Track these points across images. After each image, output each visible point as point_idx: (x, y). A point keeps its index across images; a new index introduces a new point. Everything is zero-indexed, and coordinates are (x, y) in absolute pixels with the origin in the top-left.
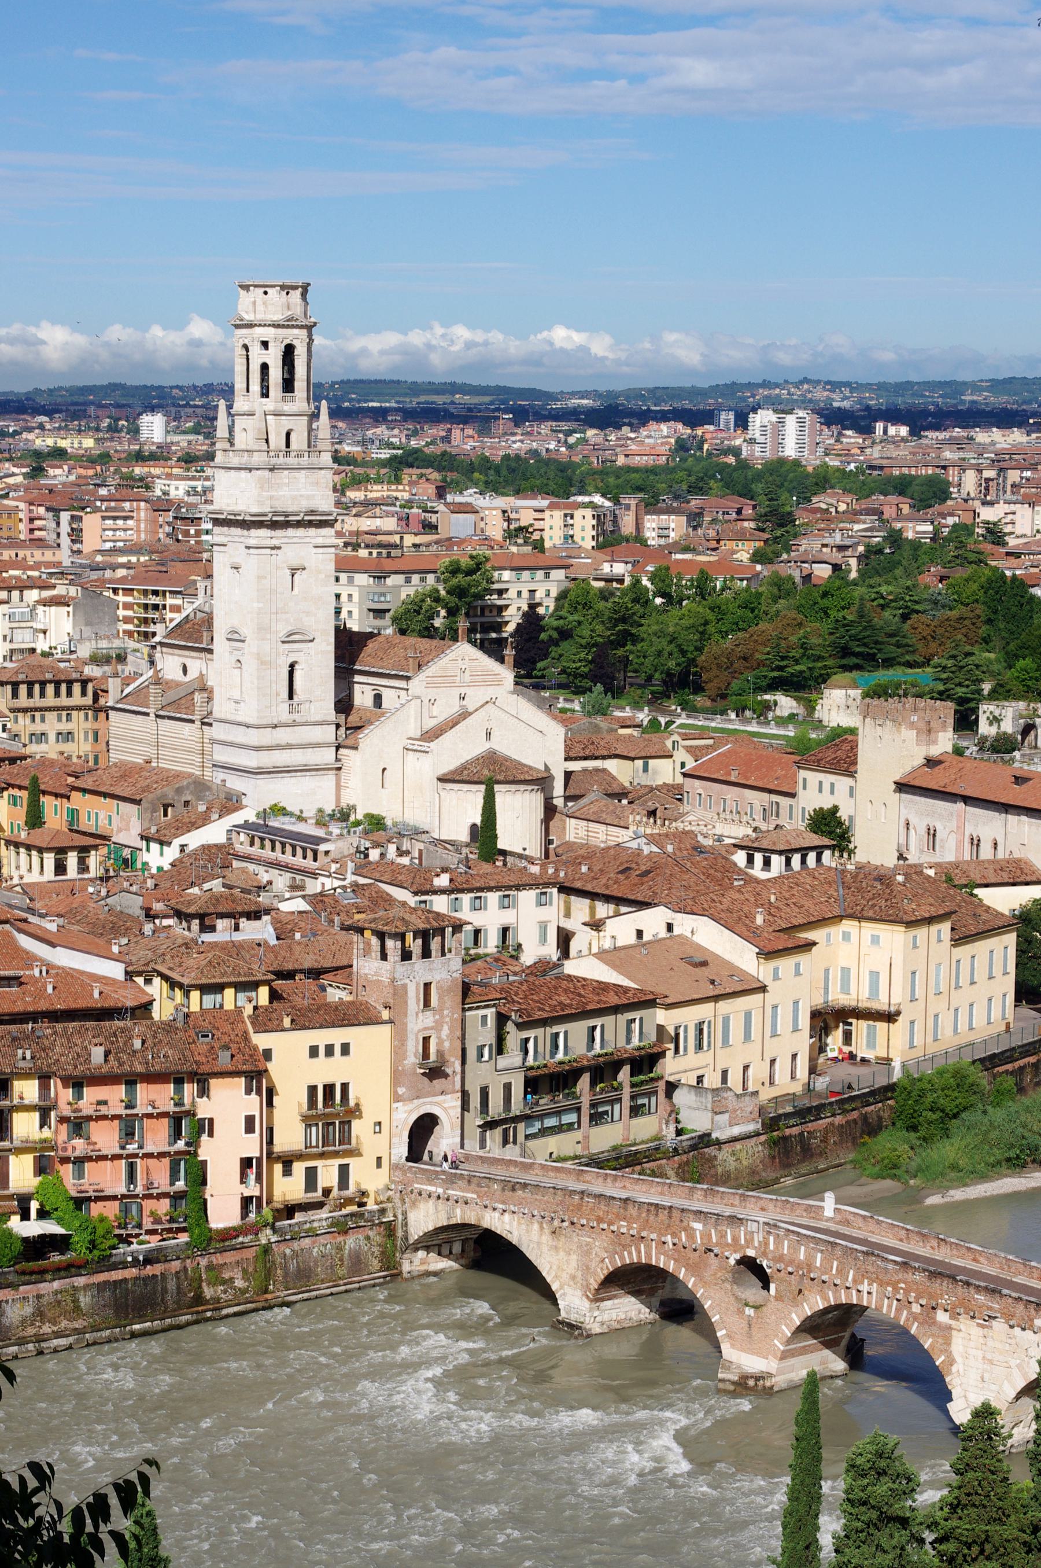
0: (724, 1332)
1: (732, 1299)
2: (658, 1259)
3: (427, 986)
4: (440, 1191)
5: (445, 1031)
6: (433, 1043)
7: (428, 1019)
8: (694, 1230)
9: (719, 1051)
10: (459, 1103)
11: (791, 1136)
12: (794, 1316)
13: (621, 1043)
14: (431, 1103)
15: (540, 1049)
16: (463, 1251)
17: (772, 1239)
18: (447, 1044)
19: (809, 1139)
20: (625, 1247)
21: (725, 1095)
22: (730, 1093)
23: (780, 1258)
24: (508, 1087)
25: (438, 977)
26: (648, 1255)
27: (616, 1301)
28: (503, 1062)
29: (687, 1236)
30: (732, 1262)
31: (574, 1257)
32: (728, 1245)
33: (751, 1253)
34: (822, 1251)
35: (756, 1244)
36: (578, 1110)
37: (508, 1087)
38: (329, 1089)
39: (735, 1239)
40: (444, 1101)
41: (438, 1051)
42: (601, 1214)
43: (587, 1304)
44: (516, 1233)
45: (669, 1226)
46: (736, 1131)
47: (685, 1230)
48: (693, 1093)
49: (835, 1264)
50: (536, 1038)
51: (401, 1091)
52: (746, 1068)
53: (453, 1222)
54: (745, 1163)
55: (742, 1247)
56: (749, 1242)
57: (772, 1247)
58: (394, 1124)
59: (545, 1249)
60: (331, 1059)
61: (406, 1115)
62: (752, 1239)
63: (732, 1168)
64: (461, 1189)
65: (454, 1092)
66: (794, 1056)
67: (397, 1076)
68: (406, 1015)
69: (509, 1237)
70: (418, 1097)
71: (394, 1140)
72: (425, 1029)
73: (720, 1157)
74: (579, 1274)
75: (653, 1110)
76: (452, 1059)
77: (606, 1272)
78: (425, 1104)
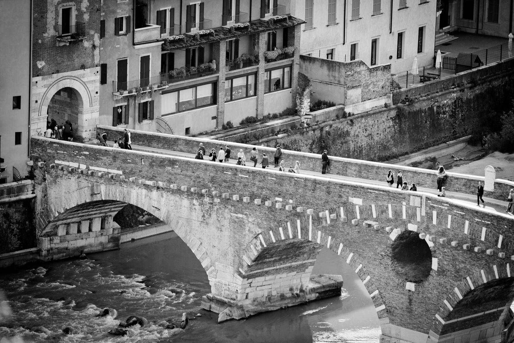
0: (383, 307)
1: (392, 274)
2: (314, 235)
4: (83, 167)
6: (74, 14)
8: (353, 205)
9: (349, 24)
10: (98, 77)
11: (420, 111)
12: (456, 290)
13: (255, 16)
14: (71, 77)
15: (177, 22)
17: (435, 213)
18: (86, 17)
19: (438, 113)
20: (279, 223)
21: (358, 69)
22: (362, 68)
23: (443, 234)
24: (145, 61)
26: (305, 230)
27: (268, 278)
28: (141, 34)
29: (346, 211)
30: (394, 236)
31: (227, 233)
32: (389, 220)
33: (412, 227)
34: (487, 226)
35: (419, 219)
36: (215, 85)
37: (145, 61)
39: (397, 214)
40: (83, 76)
41: (77, 23)
42: (255, 189)
43: (240, 280)
44: (164, 210)
45: (327, 202)
46: (368, 106)
47: (345, 204)
48: (325, 67)
49: (501, 238)
50: (172, 11)
51: (41, 64)
52: (374, 42)
53: (97, 198)
54: (376, 138)
55: (405, 223)
56: (412, 216)
57: (435, 222)
58: (33, 99)
59: (196, 224)
62: (414, 215)
63: (364, 144)
64: (105, 165)
66: (421, 30)
69: (156, 214)
70: (58, 72)
71: (34, 115)
73: (352, 133)
74: (231, 251)
75: (286, 85)
76: (92, 32)
77: (259, 248)
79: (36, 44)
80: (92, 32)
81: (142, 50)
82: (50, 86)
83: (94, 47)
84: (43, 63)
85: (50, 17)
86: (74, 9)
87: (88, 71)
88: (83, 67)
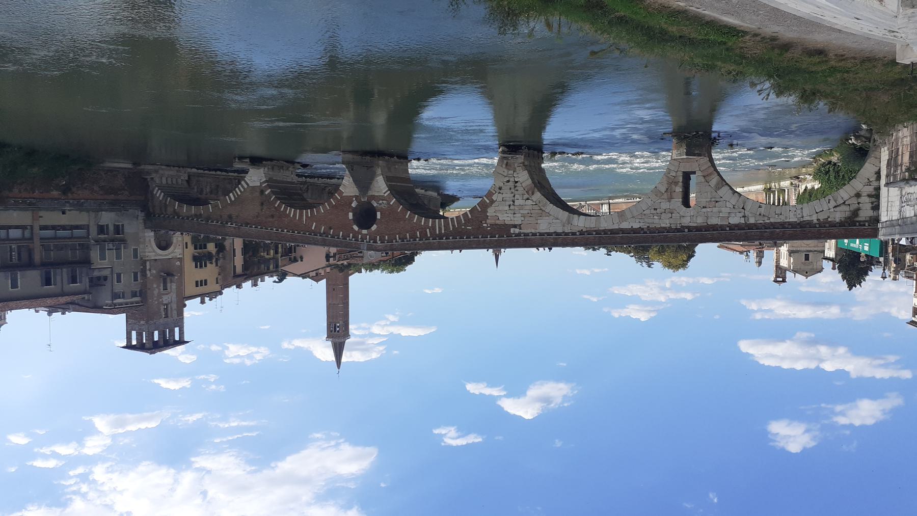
3: (167, 316)
5: (156, 292)
6: (162, 288)
7: (165, 299)
14: (162, 255)
16: (161, 178)
25: (161, 321)
37: (103, 258)
38: (201, 267)
60: (201, 279)
61: (175, 251)
67: (181, 269)
72: (167, 294)
76: (151, 278)
78: (165, 255)
79: (181, 274)
80: (151, 278)
81: (105, 263)
82: (172, 252)
83: (150, 270)
85: (174, 286)
86: (162, 290)
87: (153, 258)
88: (156, 260)
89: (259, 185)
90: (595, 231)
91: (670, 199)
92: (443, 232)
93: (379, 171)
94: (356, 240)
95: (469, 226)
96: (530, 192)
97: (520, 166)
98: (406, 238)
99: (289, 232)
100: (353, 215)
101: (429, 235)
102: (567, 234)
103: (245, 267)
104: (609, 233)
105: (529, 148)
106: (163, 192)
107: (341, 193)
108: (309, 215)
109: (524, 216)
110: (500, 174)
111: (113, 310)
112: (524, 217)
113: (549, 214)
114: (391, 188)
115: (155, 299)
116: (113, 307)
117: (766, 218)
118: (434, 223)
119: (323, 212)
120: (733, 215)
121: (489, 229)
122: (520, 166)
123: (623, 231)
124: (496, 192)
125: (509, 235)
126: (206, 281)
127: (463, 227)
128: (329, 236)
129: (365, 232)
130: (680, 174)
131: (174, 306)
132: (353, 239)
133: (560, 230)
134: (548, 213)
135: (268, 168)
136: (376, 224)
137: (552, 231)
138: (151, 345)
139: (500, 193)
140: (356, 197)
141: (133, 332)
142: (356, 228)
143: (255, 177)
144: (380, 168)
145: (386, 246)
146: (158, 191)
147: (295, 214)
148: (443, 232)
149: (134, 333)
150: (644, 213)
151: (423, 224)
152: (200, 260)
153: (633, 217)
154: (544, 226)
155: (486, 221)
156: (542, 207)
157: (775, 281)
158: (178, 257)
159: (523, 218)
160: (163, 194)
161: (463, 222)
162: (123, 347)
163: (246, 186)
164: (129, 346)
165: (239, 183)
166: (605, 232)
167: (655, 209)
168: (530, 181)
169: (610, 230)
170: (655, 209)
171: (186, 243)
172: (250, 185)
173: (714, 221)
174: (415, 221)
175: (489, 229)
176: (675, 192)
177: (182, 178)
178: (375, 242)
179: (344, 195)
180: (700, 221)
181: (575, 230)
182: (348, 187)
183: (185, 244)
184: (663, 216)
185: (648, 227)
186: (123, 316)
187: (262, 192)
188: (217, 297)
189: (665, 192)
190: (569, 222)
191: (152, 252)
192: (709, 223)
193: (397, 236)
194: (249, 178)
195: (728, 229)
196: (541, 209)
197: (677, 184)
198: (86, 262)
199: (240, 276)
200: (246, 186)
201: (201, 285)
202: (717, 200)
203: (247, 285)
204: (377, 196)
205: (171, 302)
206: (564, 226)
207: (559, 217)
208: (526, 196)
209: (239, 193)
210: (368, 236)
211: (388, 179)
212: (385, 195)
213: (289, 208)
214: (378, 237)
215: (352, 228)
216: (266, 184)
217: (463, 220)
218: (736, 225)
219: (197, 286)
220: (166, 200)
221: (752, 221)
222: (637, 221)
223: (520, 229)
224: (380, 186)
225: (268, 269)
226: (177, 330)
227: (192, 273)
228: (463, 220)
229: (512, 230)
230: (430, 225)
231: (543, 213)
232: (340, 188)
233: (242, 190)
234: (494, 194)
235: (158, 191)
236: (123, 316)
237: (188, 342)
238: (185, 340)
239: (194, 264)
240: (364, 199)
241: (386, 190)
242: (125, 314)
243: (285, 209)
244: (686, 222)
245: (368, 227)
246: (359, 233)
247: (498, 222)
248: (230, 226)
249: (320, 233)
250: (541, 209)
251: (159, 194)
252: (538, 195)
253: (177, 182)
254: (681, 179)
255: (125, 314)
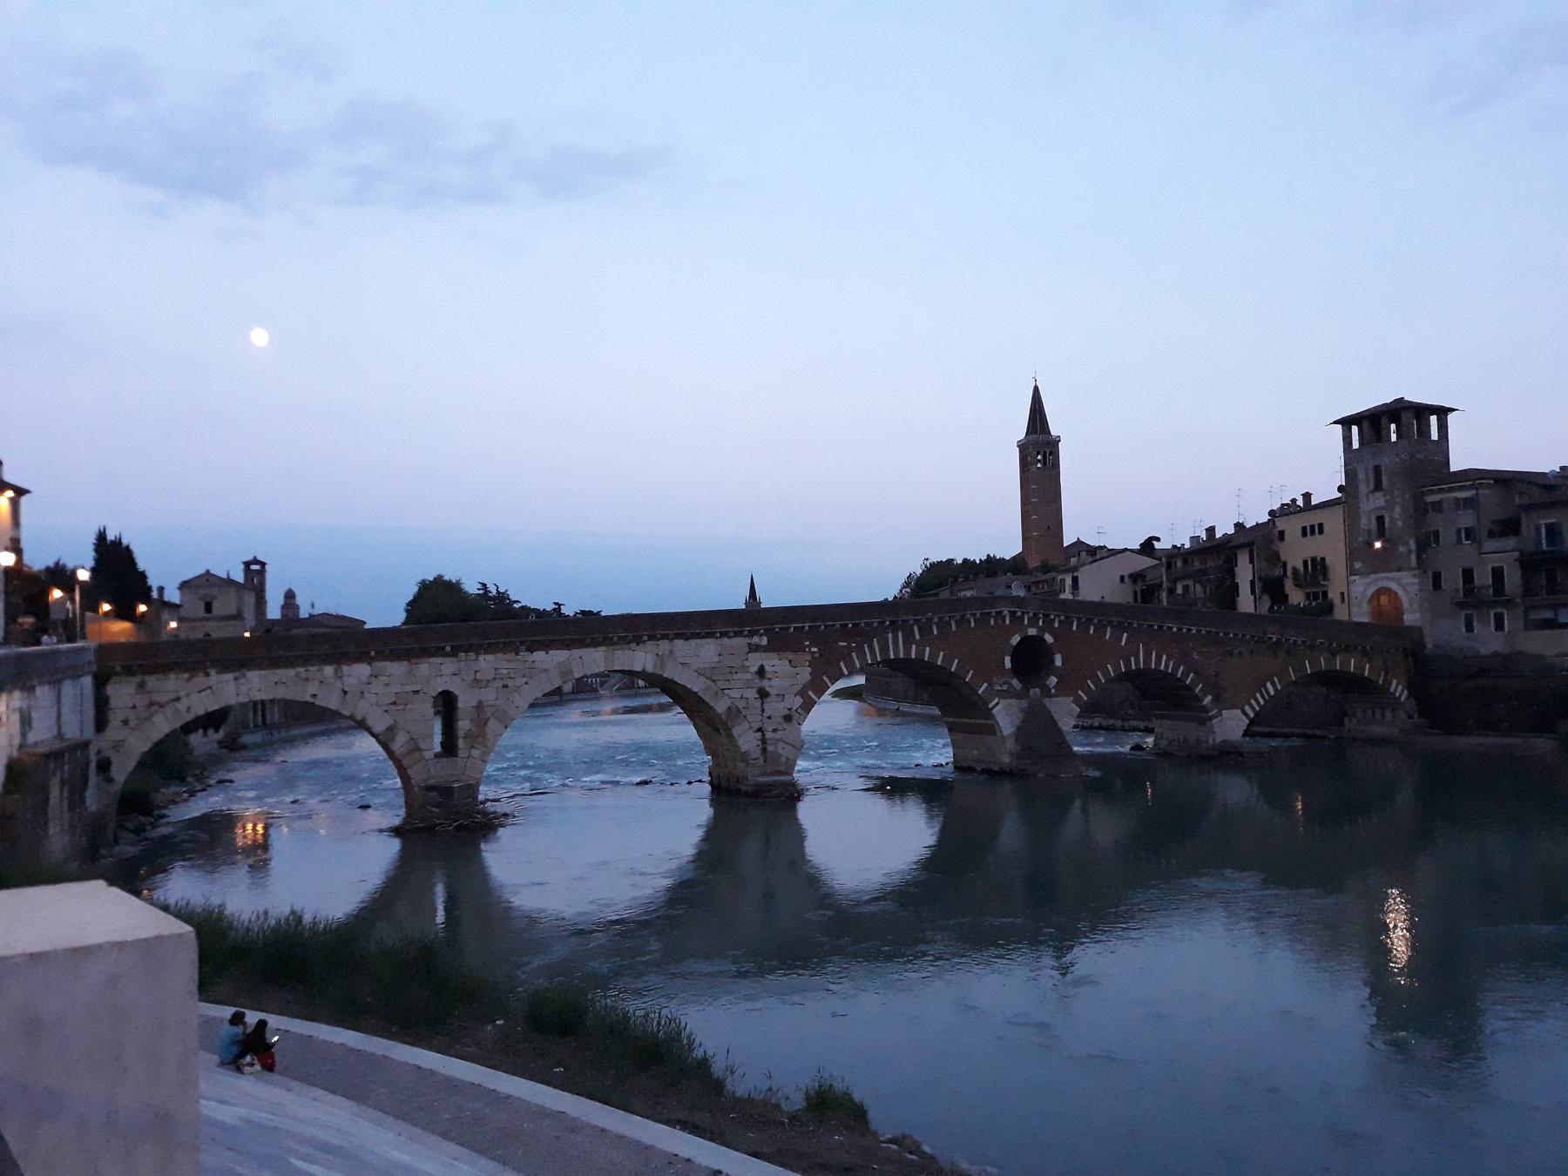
5: (1398, 510)
6: (1387, 520)
7: (1379, 500)
14: (1388, 579)
24: (1498, 574)
37: (1498, 574)
38: (1314, 560)
51: (1358, 565)
58: (1353, 595)
61: (1363, 587)
65: (1409, 569)
67: (1351, 555)
68: (1356, 497)
72: (1376, 509)
78: (1382, 578)
80: (1407, 538)
81: (1493, 561)
84: (1360, 565)
85: (1364, 523)
87: (1405, 573)
88: (1399, 570)
89: (1224, 712)
90: (614, 644)
91: (480, 706)
92: (890, 635)
93: (1010, 744)
94: (1047, 615)
95: (842, 646)
96: (734, 711)
97: (755, 759)
98: (956, 622)
99: (1168, 627)
100: (1053, 661)
101: (916, 628)
102: (664, 637)
103: (1231, 563)
104: (588, 641)
105: (738, 792)
106: (1391, 693)
107: (1077, 701)
108: (1132, 659)
109: (745, 669)
110: (788, 744)
111: (1474, 477)
112: (743, 666)
113: (699, 672)
114: (988, 714)
115: (1399, 499)
116: (1477, 482)
117: (302, 676)
118: (907, 650)
119: (1109, 666)
120: (364, 679)
121: (807, 643)
122: (755, 759)
123: (567, 645)
124: (796, 711)
125: (768, 632)
126: (1304, 534)
127: (854, 645)
128: (1096, 621)
129: (1032, 632)
130: (462, 753)
131: (1363, 489)
132: (1052, 617)
133: (679, 643)
134: (699, 674)
135: (1207, 742)
136: (1011, 645)
137: (693, 643)
138: (1406, 417)
139: (789, 709)
140: (1050, 696)
141: (1436, 439)
142: (1049, 638)
143: (1231, 725)
144: (1008, 750)
145: (992, 607)
146: (1400, 695)
147: (1159, 658)
148: (890, 635)
149: (1435, 436)
150: (525, 680)
151: (928, 649)
152: (1317, 569)
153: (546, 671)
154: (707, 651)
155: (813, 657)
156: (713, 684)
157: (263, 564)
158: (1356, 577)
159: (747, 663)
160: (1392, 690)
161: (854, 654)
162: (1454, 410)
163: (1247, 709)
164: (1442, 412)
165: (1257, 714)
166: (595, 644)
167: (505, 686)
168: (736, 732)
169: (588, 646)
170: (505, 686)
171: (1343, 601)
172: (1240, 711)
173: (397, 668)
174: (942, 653)
175: (807, 643)
176: (472, 720)
177: (1354, 721)
178: (1012, 614)
179: (1072, 698)
180: (424, 667)
181: (651, 645)
182: (1065, 712)
183: (1346, 600)
184: (491, 676)
185: (517, 654)
186: (1456, 465)
187: (1217, 699)
188: (1279, 506)
189: (489, 719)
190: (660, 657)
191: (1408, 584)
192: (405, 663)
193: (973, 625)
194: (1241, 723)
195: (373, 653)
196: (714, 681)
197: (466, 734)
198: (1529, 564)
199: (1242, 546)
200: (1247, 709)
201: (1312, 527)
202: (393, 707)
203: (1225, 528)
204: (1011, 698)
205: (1367, 496)
206: (671, 652)
207: (680, 666)
208: (741, 705)
209: (1258, 695)
210: (1026, 622)
211: (992, 730)
212: (996, 700)
213: (1170, 671)
214: (1008, 622)
215: (1055, 638)
216: (1210, 714)
217: (855, 657)
218: (358, 660)
219: (1321, 526)
220: (1385, 680)
221: (329, 670)
222: (536, 665)
223: (749, 644)
224: (1006, 716)
225: (1185, 562)
226: (1356, 445)
227: (1332, 547)
228: (855, 657)
229: (764, 641)
230: (914, 646)
231: (710, 674)
232: (1079, 710)
233: (1253, 701)
234: (800, 707)
235: (1400, 695)
236: (1456, 465)
237: (1335, 422)
238: (1340, 426)
239: (1328, 562)
240: (1035, 692)
241: (996, 709)
242: (1451, 470)
243: (1176, 668)
244: (448, 665)
245: (1026, 640)
246: (1042, 630)
247: (790, 655)
248: (1274, 634)
249: (1112, 627)
250: (714, 681)
251: (1398, 689)
252: (720, 707)
253: (1364, 711)
254: (461, 743)
255: (1451, 470)
